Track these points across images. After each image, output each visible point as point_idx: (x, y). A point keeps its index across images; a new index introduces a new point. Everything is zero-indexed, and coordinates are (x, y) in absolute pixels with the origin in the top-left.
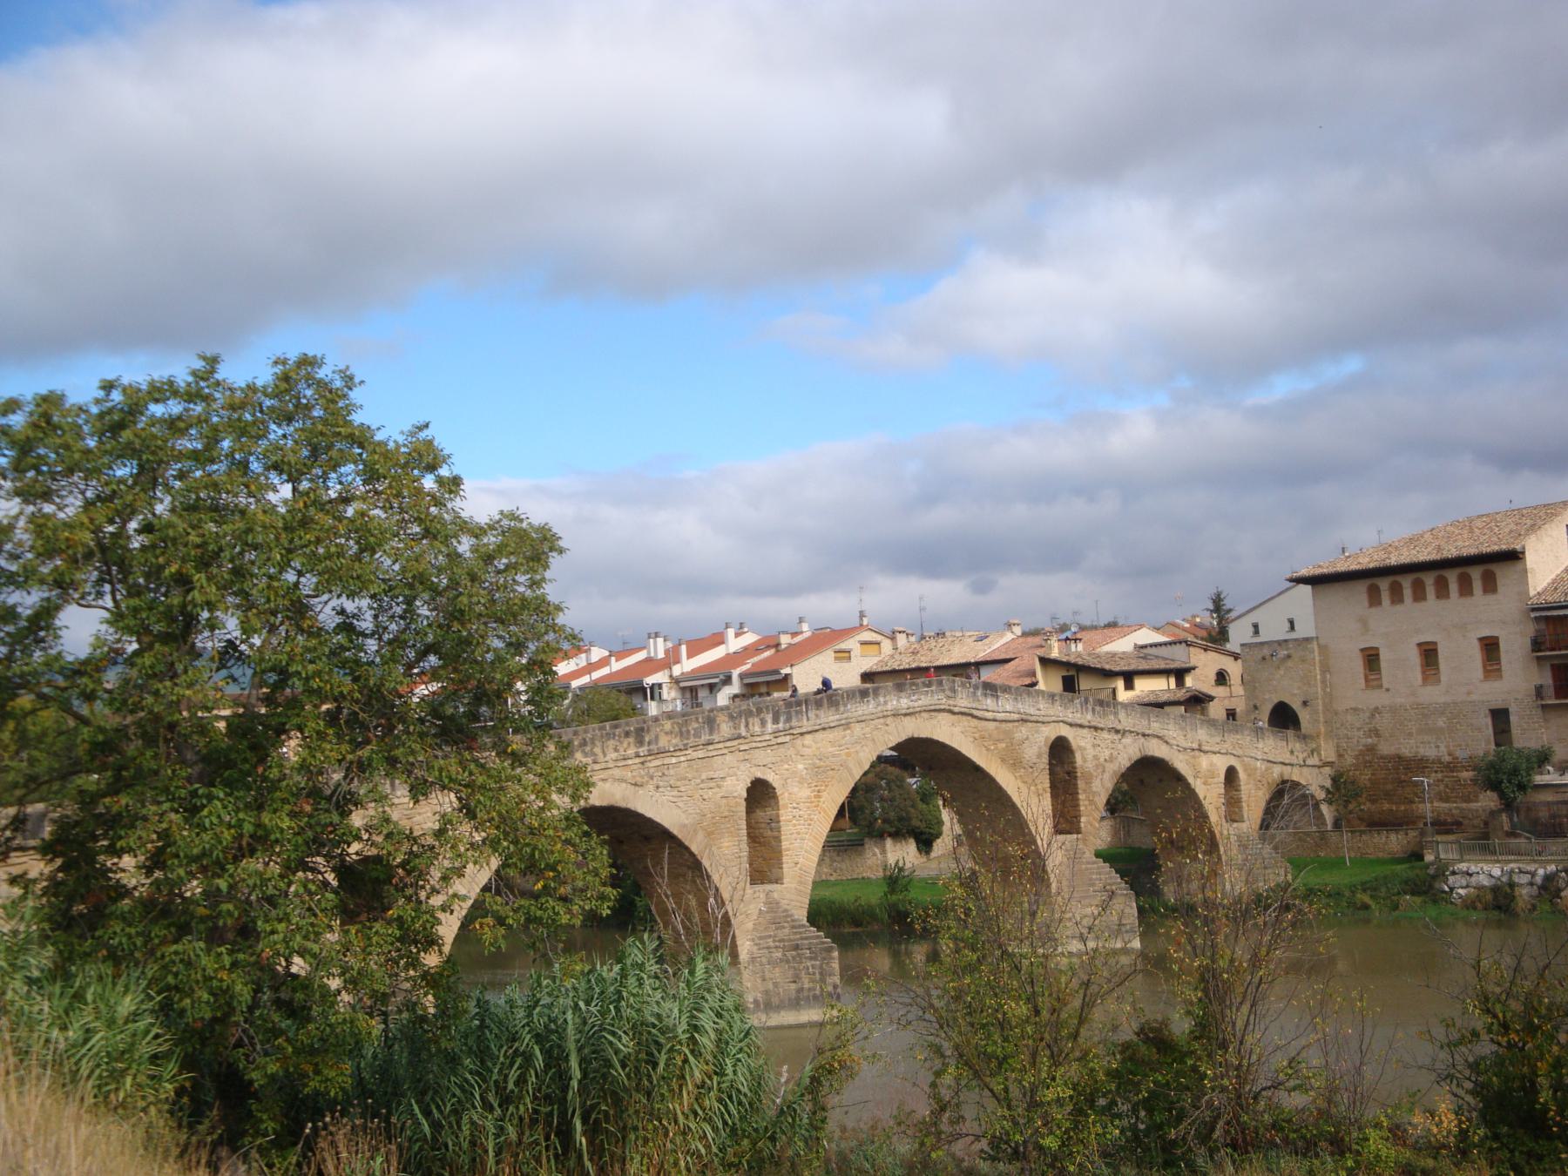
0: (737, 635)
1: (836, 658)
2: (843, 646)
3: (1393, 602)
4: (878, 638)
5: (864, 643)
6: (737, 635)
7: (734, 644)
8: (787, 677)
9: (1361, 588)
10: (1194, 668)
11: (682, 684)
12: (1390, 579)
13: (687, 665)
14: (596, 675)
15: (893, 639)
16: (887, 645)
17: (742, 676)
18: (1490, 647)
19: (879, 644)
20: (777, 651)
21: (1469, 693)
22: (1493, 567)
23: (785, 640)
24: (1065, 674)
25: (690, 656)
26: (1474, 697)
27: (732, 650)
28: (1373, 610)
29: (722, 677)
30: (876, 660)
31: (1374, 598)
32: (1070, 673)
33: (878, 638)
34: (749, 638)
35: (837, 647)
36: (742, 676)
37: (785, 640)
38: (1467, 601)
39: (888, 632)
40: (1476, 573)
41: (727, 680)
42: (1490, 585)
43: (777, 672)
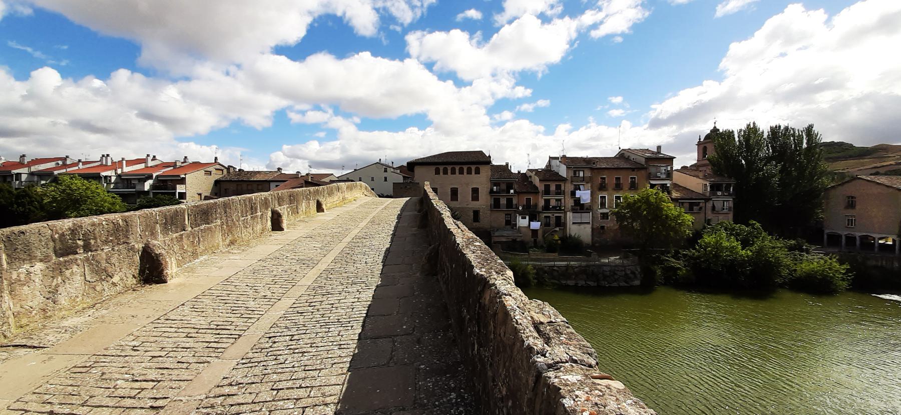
2: (208, 169)
3: (459, 174)
4: (223, 168)
5: (216, 169)
6: (152, 160)
7: (151, 163)
8: (184, 179)
9: (433, 168)
11: (122, 177)
12: (452, 166)
13: (127, 169)
17: (157, 176)
18: (475, 191)
19: (222, 170)
20: (174, 168)
21: (468, 205)
25: (126, 166)
26: (468, 206)
27: (149, 165)
29: (146, 176)
30: (221, 176)
33: (223, 168)
35: (206, 170)
37: (179, 164)
39: (227, 166)
40: (473, 167)
41: (150, 177)
42: (478, 172)
43: (179, 176)
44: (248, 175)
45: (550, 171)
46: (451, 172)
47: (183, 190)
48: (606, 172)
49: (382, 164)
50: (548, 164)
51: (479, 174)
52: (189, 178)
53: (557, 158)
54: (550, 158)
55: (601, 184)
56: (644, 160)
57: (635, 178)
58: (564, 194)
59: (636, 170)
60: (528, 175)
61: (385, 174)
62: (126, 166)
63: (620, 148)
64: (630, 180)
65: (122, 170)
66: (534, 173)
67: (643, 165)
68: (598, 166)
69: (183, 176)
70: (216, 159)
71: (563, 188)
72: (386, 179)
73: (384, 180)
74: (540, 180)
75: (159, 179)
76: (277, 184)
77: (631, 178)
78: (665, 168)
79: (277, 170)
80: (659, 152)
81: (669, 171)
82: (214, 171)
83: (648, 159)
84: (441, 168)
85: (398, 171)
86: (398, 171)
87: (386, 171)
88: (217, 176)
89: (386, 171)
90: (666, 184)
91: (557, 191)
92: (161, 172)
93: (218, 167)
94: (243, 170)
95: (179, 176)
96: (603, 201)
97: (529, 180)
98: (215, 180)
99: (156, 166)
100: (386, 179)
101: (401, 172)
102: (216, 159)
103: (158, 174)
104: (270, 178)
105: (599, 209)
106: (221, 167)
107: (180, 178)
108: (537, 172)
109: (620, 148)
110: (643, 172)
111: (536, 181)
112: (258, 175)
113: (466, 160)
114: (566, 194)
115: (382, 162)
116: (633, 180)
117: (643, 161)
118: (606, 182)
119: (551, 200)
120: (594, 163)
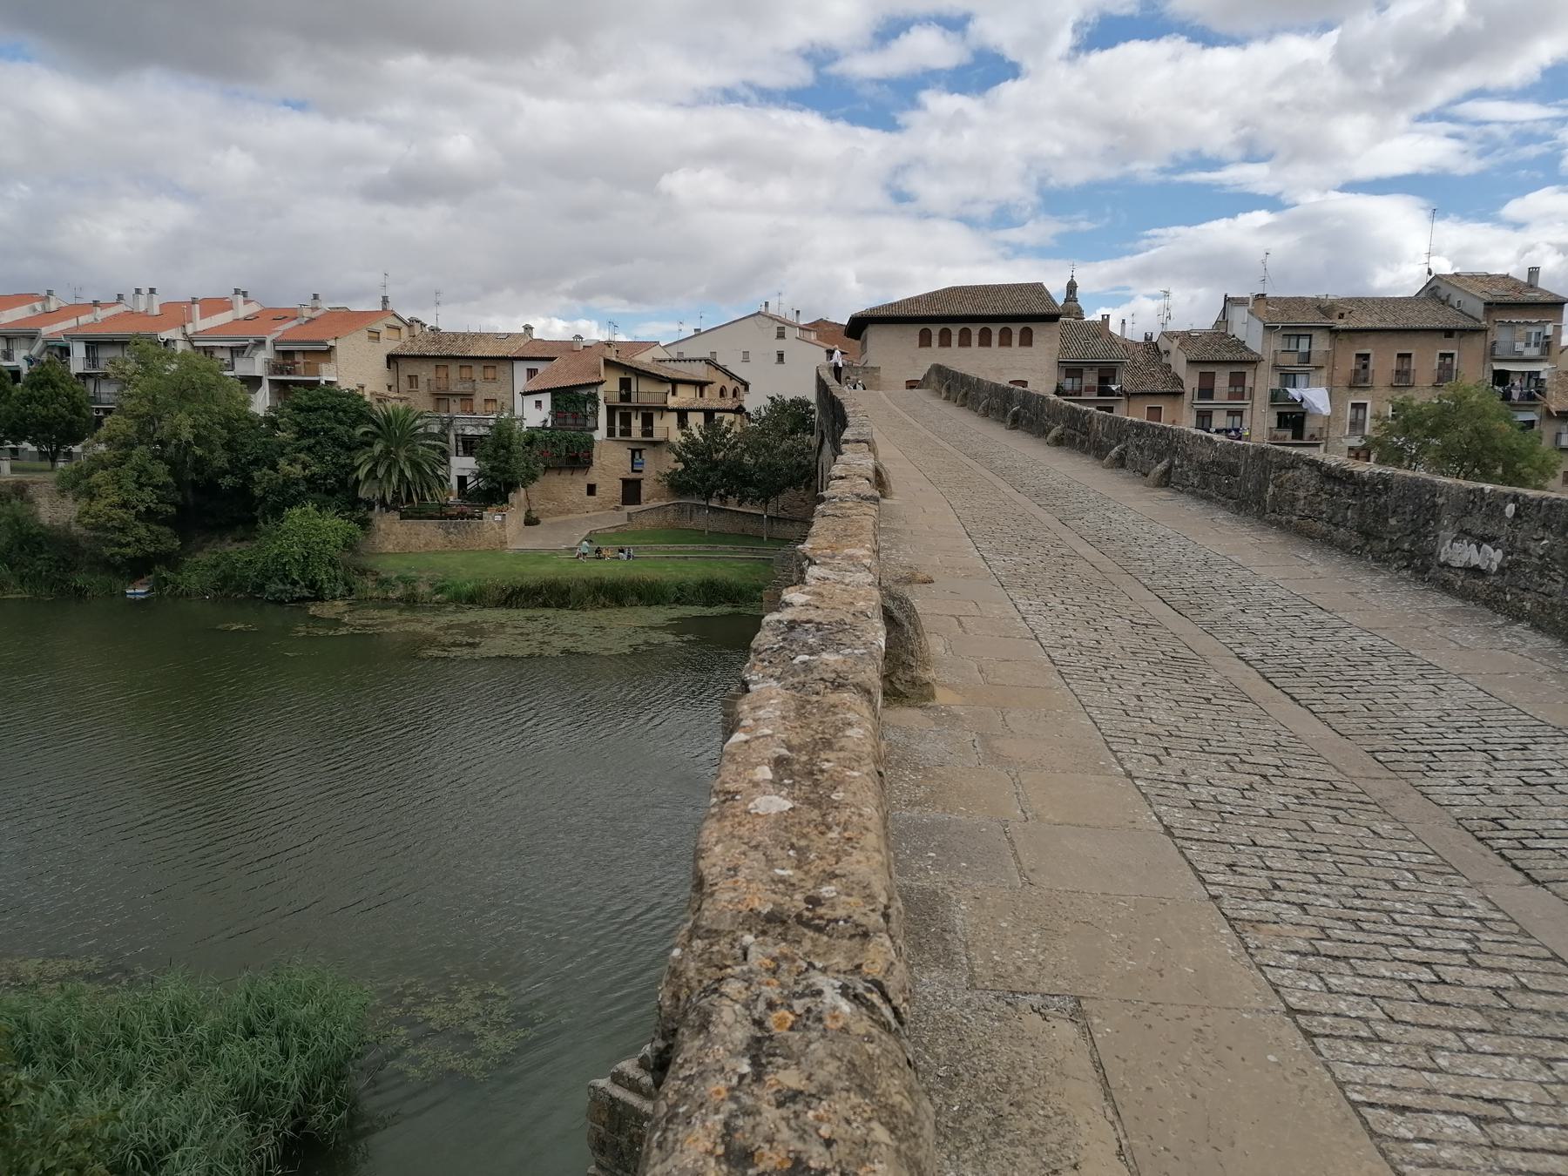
0: (246, 302)
1: (370, 338)
2: (375, 327)
3: (981, 344)
4: (400, 324)
6: (246, 302)
7: (243, 310)
8: (331, 349)
9: (915, 330)
10: (712, 383)
11: (196, 344)
12: (962, 326)
13: (200, 324)
14: (83, 319)
15: (410, 326)
16: (405, 329)
17: (275, 343)
22: (1033, 326)
23: (307, 314)
24: (623, 376)
25: (202, 317)
27: (241, 315)
28: (924, 350)
31: (925, 340)
32: (627, 376)
33: (400, 324)
34: (253, 308)
36: (275, 343)
38: (1005, 350)
40: (1016, 329)
41: (260, 343)
42: (1027, 339)
44: (460, 342)
45: (1225, 335)
46: (980, 339)
47: (332, 376)
48: (1373, 338)
49: (770, 317)
50: (1221, 319)
51: (1030, 344)
52: (343, 348)
53: (1241, 302)
54: (1227, 300)
55: (1356, 372)
56: (1481, 307)
57: (1451, 355)
58: (1251, 397)
59: (1456, 333)
60: (1162, 349)
61: (780, 345)
62: (202, 317)
63: (1430, 272)
64: (1437, 360)
65: (195, 326)
66: (1177, 342)
67: (1477, 320)
68: (1353, 324)
69: (331, 343)
70: (385, 300)
71: (1249, 383)
72: (781, 356)
73: (776, 360)
74: (1190, 362)
75: (278, 348)
76: (532, 365)
77: (1443, 356)
78: (1538, 329)
79: (522, 331)
80: (1531, 286)
81: (1547, 337)
82: (384, 333)
83: (1490, 307)
84: (935, 330)
85: (813, 336)
86: (813, 336)
87: (781, 335)
88: (390, 345)
89: (781, 335)
90: (1538, 373)
91: (1232, 390)
92: (279, 334)
93: (393, 321)
94: (439, 330)
95: (323, 343)
96: (1360, 417)
97: (1164, 360)
98: (387, 352)
99: (256, 317)
100: (781, 356)
101: (819, 337)
102: (385, 300)
103: (274, 336)
104: (513, 353)
105: (1345, 437)
106: (397, 321)
107: (325, 348)
108: (1186, 338)
109: (1430, 272)
110: (1478, 341)
111: (1179, 363)
112: (482, 343)
113: (999, 311)
114: (1256, 398)
115: (772, 311)
116: (1448, 360)
117: (1478, 309)
118: (1371, 367)
119: (1215, 414)
120: (1341, 316)
